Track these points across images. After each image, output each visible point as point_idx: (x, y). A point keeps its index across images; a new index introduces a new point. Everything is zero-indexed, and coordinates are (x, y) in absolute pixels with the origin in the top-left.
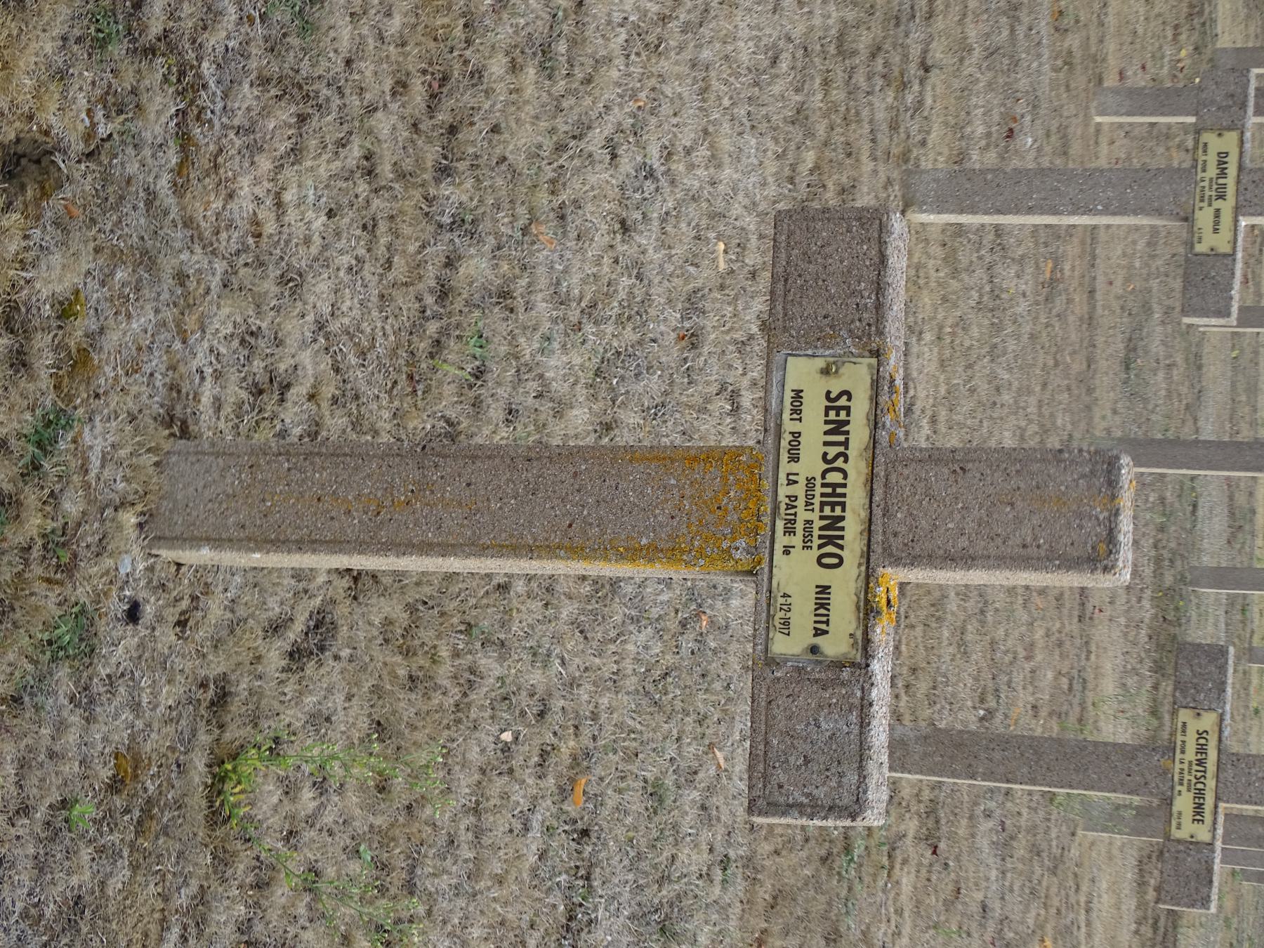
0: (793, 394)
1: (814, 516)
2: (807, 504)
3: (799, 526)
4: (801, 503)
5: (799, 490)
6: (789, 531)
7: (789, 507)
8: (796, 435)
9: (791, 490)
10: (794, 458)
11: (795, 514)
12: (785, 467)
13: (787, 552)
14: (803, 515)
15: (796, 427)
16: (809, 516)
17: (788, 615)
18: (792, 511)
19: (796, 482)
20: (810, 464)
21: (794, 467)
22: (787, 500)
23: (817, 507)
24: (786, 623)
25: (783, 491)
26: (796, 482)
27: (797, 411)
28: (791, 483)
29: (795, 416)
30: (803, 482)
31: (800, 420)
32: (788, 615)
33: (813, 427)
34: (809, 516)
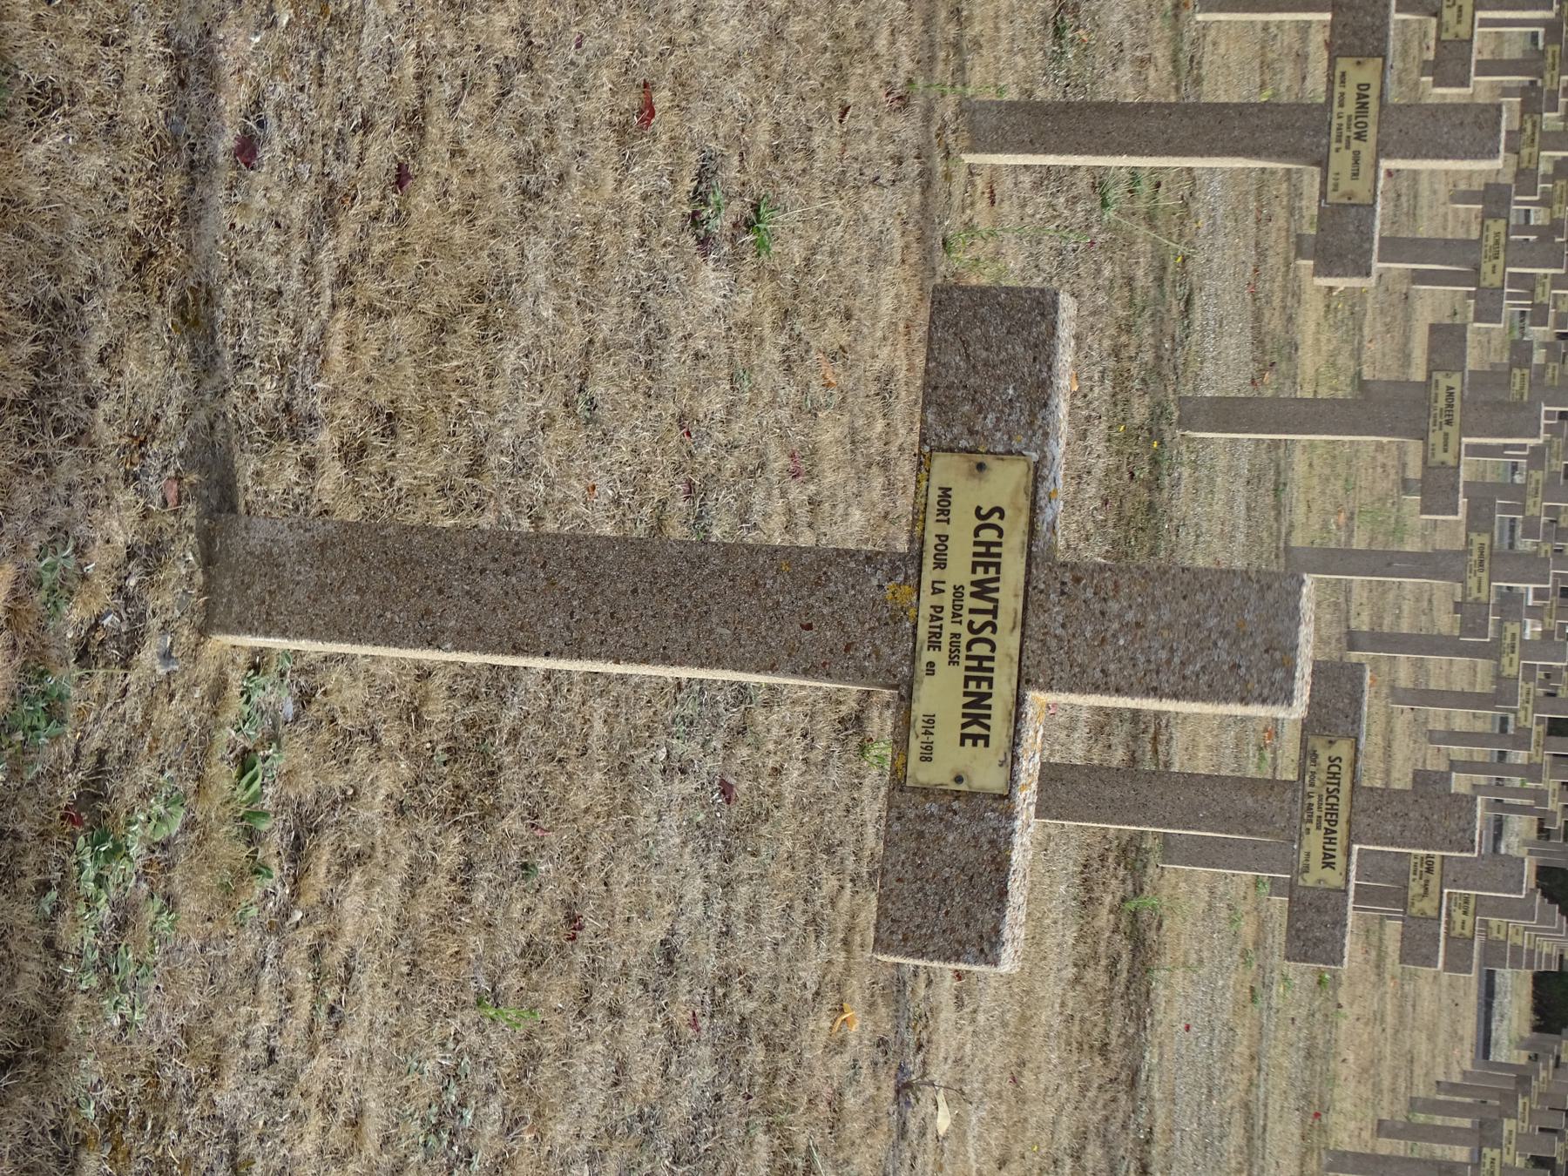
0: (940, 493)
1: (963, 629)
2: (955, 615)
3: (945, 640)
4: (947, 614)
5: (947, 600)
7: (933, 618)
8: (943, 539)
10: (941, 564)
11: (941, 627)
12: (929, 574)
14: (949, 628)
15: (940, 529)
16: (957, 629)
18: (938, 623)
20: (959, 571)
25: (927, 599)
27: (944, 511)
28: (936, 591)
29: (942, 517)
30: (949, 591)
31: (948, 521)
34: (957, 629)
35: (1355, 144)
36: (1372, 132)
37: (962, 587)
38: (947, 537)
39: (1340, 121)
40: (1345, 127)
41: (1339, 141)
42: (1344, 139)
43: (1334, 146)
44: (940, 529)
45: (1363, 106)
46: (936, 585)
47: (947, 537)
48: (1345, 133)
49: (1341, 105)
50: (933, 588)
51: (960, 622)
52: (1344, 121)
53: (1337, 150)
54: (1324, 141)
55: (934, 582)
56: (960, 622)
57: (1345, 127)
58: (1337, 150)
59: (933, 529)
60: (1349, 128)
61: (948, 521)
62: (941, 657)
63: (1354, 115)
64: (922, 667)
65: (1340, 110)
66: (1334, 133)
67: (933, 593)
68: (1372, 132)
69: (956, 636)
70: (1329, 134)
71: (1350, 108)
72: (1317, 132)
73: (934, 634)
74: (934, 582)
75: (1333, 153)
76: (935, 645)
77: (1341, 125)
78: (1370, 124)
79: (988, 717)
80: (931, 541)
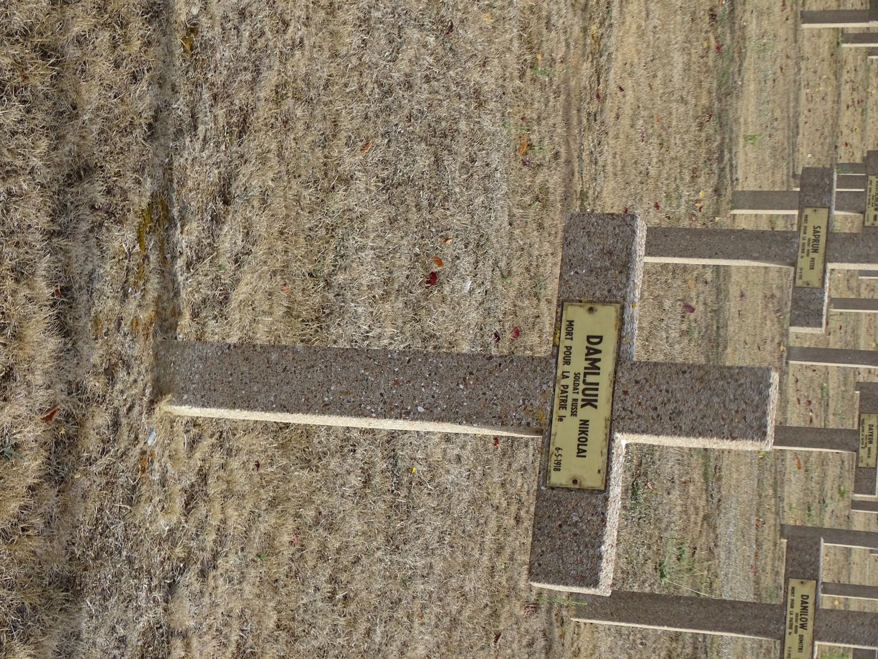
0: (567, 323)
1: (580, 397)
2: (575, 389)
4: (570, 390)
6: (563, 406)
8: (569, 348)
9: (564, 382)
11: (567, 397)
12: (562, 368)
13: (561, 419)
15: (568, 343)
16: (576, 396)
17: (559, 458)
19: (568, 377)
21: (566, 368)
22: (562, 388)
23: (580, 391)
24: (559, 463)
26: (568, 377)
27: (570, 333)
29: (568, 337)
30: (572, 376)
31: (572, 339)
32: (559, 458)
33: (579, 346)
35: (800, 631)
36: (810, 624)
37: (579, 374)
38: (571, 347)
39: (791, 616)
40: (794, 620)
41: (791, 628)
42: (794, 627)
43: (788, 631)
44: (568, 343)
45: (805, 609)
46: (565, 374)
47: (571, 347)
48: (794, 624)
49: (792, 607)
50: (563, 375)
51: (578, 393)
52: (794, 616)
53: (790, 633)
54: (782, 628)
55: (563, 372)
56: (578, 393)
57: (794, 620)
58: (790, 633)
59: (564, 343)
60: (796, 621)
61: (572, 339)
62: (567, 412)
63: (800, 613)
64: (555, 416)
65: (791, 609)
66: (788, 623)
67: (563, 378)
68: (810, 624)
69: (576, 400)
70: (785, 623)
71: (797, 609)
72: (778, 621)
73: (563, 401)
74: (563, 372)
75: (787, 635)
76: (563, 406)
77: (792, 618)
78: (809, 620)
79: (596, 401)
80: (562, 349)
